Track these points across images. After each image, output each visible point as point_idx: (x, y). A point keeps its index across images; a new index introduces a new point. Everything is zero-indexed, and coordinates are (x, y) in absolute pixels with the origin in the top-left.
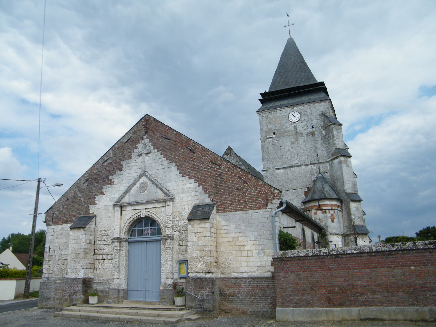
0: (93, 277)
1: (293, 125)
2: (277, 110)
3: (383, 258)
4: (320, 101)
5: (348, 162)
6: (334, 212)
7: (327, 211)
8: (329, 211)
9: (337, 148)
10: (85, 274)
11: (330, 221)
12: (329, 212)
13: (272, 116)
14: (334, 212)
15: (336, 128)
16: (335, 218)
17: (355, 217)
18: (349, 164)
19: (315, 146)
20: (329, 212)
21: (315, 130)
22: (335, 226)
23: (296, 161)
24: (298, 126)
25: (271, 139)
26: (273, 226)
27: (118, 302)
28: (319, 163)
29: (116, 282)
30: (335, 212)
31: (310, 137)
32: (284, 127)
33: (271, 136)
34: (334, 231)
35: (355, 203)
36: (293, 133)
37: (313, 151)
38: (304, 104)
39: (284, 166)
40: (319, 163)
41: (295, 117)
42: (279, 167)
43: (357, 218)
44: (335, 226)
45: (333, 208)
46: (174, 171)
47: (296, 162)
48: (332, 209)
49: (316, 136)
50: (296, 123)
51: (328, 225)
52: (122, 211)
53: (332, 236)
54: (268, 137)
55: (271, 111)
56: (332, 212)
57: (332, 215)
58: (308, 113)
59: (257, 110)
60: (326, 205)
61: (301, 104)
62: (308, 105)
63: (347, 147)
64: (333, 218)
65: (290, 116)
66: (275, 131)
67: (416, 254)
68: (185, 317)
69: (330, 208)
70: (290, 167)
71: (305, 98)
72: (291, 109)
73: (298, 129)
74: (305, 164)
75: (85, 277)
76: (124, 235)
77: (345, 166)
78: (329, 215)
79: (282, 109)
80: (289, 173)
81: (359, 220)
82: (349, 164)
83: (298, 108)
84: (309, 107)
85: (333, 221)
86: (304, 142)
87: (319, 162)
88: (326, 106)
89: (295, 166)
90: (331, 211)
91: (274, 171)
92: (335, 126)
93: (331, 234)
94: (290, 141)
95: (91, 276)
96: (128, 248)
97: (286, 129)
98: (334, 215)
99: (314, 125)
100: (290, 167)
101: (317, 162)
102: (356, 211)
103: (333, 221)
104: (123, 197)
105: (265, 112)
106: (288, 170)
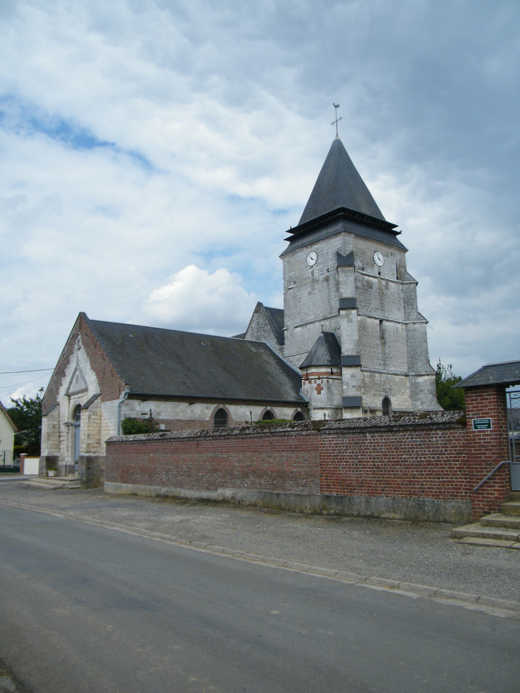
0: (58, 455)
1: (310, 271)
2: (296, 252)
3: (421, 435)
4: (334, 236)
5: (351, 315)
6: (322, 382)
7: (313, 381)
8: (315, 381)
9: (342, 297)
10: (49, 452)
11: (315, 392)
12: (315, 382)
13: (293, 260)
14: (322, 382)
15: (343, 272)
16: (322, 389)
17: (347, 387)
18: (352, 319)
19: (329, 296)
20: (315, 382)
21: (329, 275)
22: (322, 399)
23: (312, 316)
24: (315, 271)
25: (292, 290)
26: (120, 415)
27: (66, 475)
28: (332, 317)
29: (66, 459)
30: (324, 382)
31: (325, 284)
32: (303, 273)
33: (292, 287)
34: (320, 405)
35: (350, 369)
36: (310, 280)
37: (327, 302)
38: (320, 241)
39: (301, 324)
40: (332, 317)
41: (312, 259)
42: (297, 325)
43: (351, 387)
44: (322, 399)
45: (321, 377)
46: (89, 366)
47: (312, 318)
48: (319, 379)
49: (331, 282)
50: (314, 267)
51: (312, 397)
52: (69, 399)
53: (316, 411)
54: (289, 288)
55: (292, 254)
56: (319, 382)
57: (319, 385)
58: (325, 252)
59: (280, 254)
60: (312, 374)
61: (317, 241)
62: (324, 242)
63: (415, 280)
64: (319, 390)
65: (308, 259)
66: (295, 280)
67: (154, 444)
68: (67, 486)
69: (317, 377)
70: (306, 324)
71: (323, 233)
72: (310, 249)
73: (315, 274)
74: (319, 319)
75: (49, 455)
76: (71, 421)
77: (346, 321)
78: (315, 386)
79: (300, 250)
80: (305, 332)
81: (355, 389)
82: (352, 319)
83: (316, 247)
84: (325, 244)
85: (319, 393)
86: (320, 291)
87: (332, 316)
88: (341, 241)
89: (310, 323)
90: (317, 380)
91: (293, 330)
92: (342, 268)
93: (315, 409)
94: (307, 291)
95: (56, 454)
96: (74, 431)
97: (305, 276)
98: (322, 385)
99: (329, 267)
100: (306, 324)
101: (329, 316)
102: (351, 379)
103: (319, 393)
104: (69, 388)
105: (286, 256)
106: (304, 327)
